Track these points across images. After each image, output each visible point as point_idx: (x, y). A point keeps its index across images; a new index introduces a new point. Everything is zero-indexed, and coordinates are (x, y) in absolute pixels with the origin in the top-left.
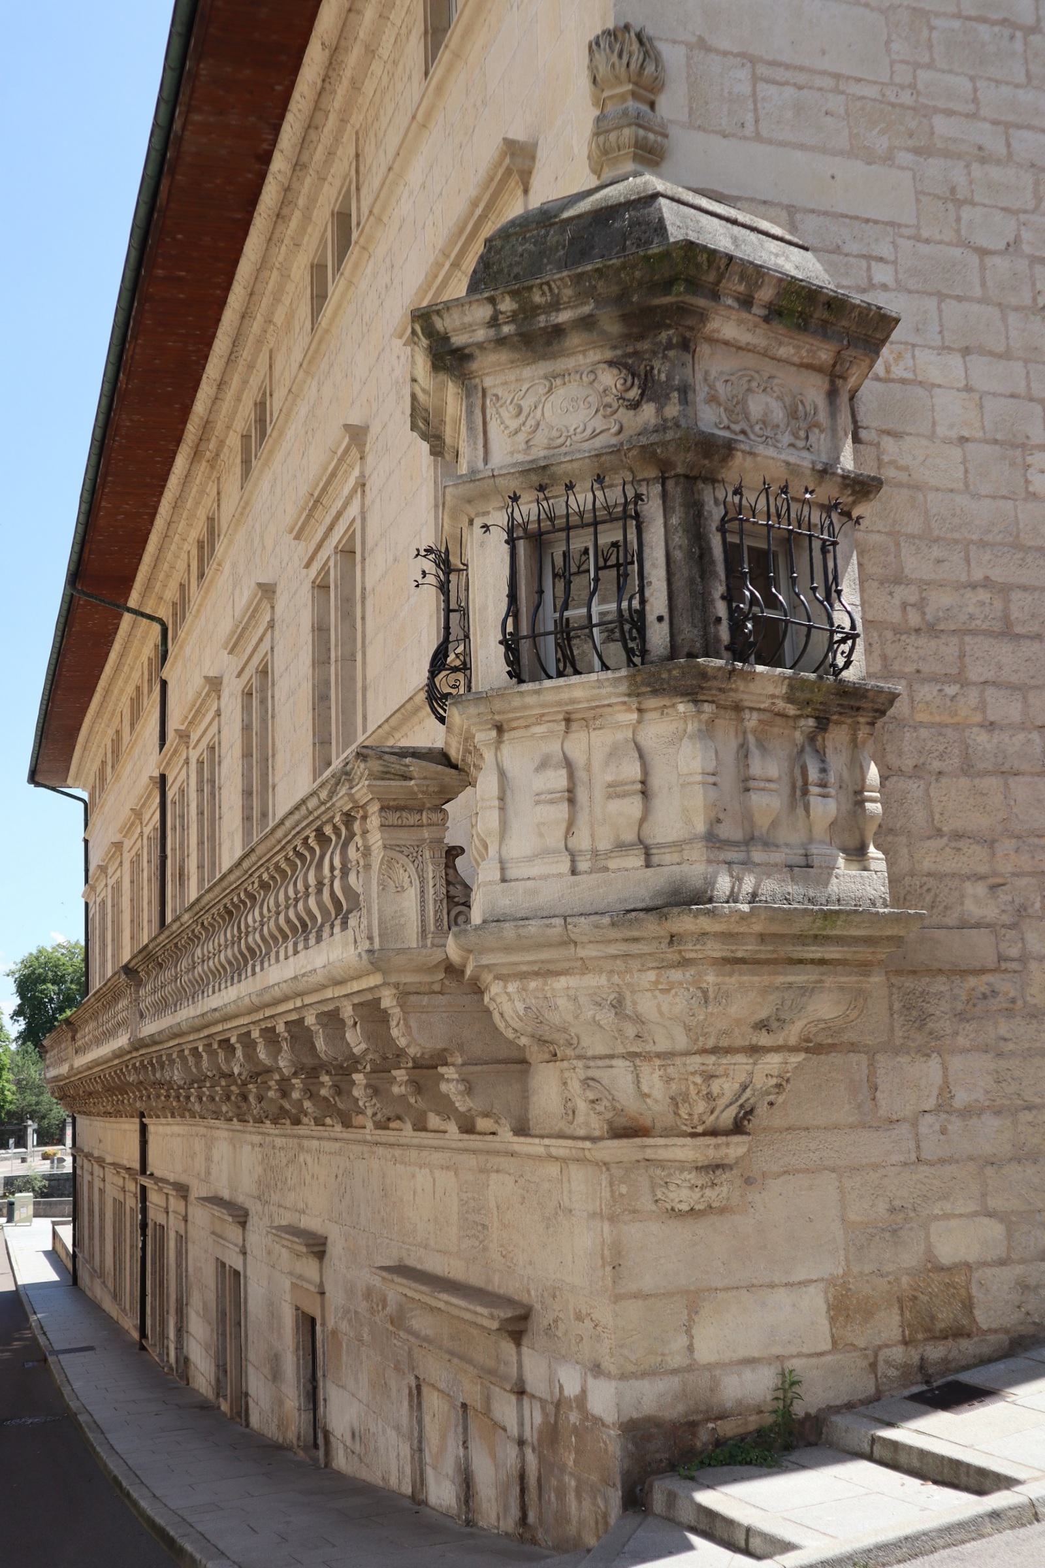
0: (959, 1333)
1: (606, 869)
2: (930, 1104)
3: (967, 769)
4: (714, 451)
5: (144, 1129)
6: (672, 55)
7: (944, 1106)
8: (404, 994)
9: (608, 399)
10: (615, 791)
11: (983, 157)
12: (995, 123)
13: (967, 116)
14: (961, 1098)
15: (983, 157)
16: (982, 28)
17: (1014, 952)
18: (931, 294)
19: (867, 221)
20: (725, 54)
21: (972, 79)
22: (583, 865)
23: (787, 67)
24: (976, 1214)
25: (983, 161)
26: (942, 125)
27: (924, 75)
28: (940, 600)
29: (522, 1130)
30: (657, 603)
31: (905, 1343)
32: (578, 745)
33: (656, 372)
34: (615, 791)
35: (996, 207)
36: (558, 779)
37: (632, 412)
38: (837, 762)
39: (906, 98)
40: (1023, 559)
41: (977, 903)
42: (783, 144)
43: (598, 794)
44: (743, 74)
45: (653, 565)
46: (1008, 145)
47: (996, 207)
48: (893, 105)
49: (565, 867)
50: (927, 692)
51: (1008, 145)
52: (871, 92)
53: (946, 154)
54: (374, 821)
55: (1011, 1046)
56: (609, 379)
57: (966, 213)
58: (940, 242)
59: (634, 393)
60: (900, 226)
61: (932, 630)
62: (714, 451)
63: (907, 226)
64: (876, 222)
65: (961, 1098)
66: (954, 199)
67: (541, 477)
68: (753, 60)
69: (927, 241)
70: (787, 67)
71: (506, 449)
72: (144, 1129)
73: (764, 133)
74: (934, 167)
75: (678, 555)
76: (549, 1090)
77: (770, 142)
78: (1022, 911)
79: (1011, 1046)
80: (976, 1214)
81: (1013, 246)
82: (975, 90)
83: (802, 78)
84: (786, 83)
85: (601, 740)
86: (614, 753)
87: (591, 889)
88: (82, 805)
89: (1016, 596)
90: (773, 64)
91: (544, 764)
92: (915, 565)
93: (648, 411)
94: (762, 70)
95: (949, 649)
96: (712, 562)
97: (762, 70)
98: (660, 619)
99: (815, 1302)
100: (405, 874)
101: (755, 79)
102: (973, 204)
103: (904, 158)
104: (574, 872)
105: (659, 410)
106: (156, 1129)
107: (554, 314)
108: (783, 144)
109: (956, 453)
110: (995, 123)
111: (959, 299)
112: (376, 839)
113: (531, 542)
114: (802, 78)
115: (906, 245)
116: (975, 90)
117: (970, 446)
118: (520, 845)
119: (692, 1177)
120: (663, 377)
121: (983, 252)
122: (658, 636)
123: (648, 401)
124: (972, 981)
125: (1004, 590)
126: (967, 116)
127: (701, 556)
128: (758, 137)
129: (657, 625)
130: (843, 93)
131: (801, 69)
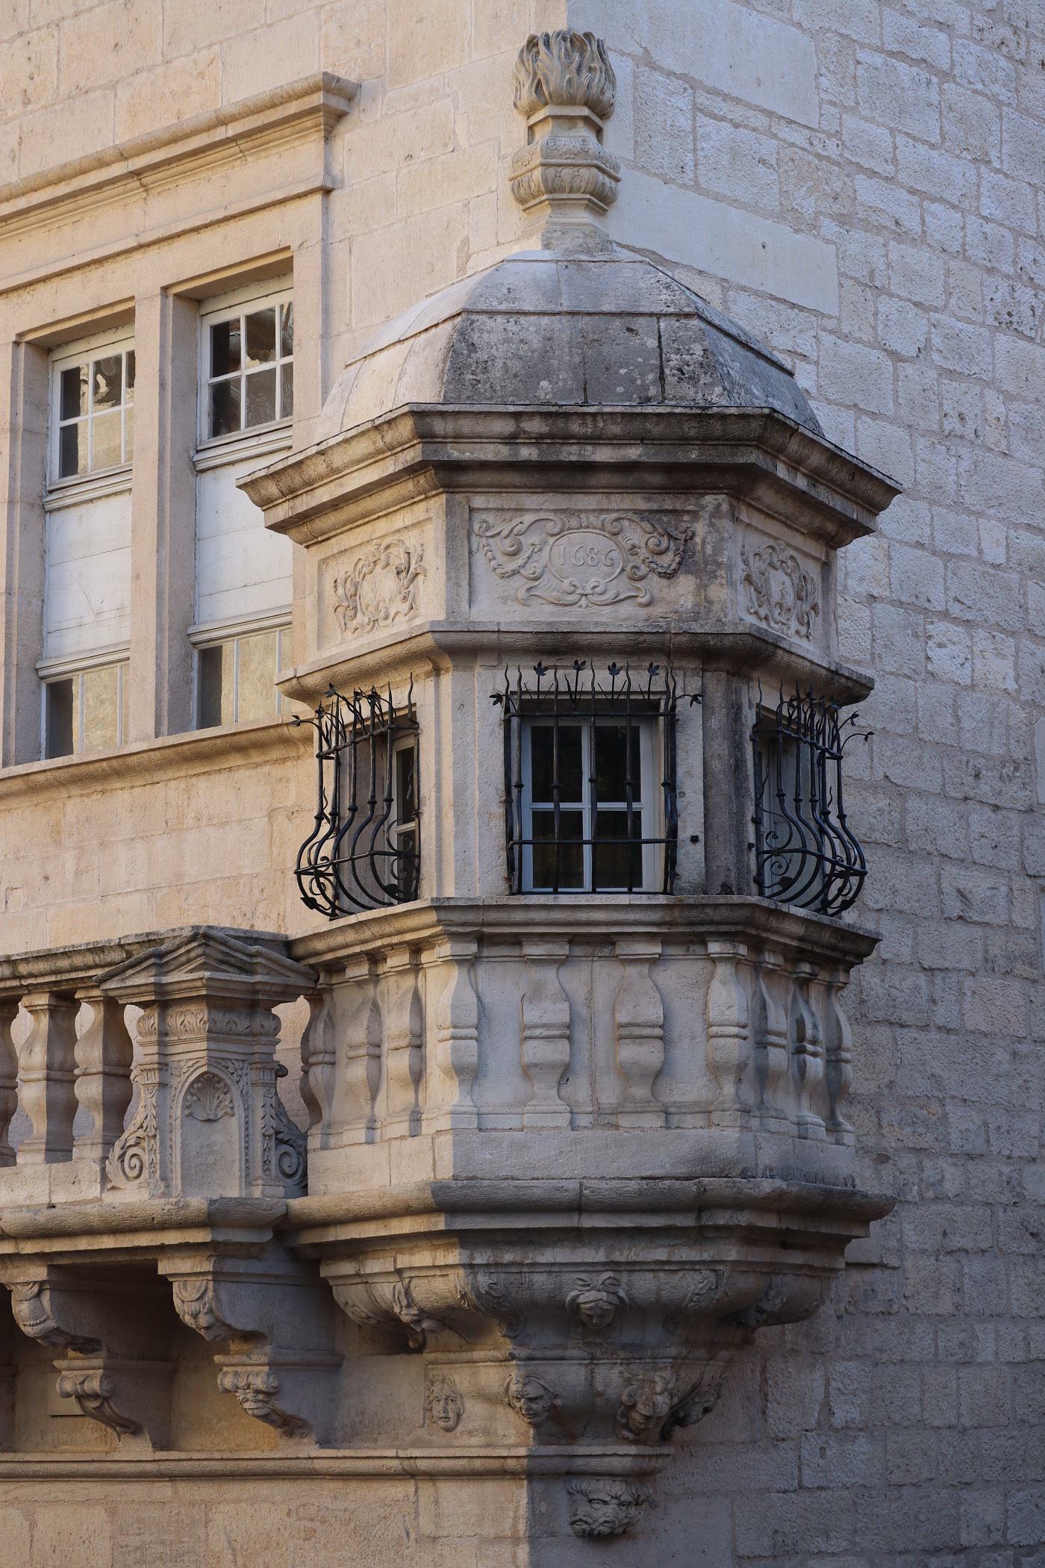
1: (617, 1127)
2: (812, 1422)
7: (826, 1424)
9: (637, 561)
11: (899, 232)
12: (913, 191)
13: (887, 179)
14: (839, 1417)
15: (899, 232)
16: (902, 67)
17: (893, 1244)
18: (848, 407)
19: (793, 306)
20: (670, 74)
21: (892, 131)
22: (583, 1120)
23: (726, 97)
24: (846, 1552)
25: (900, 238)
26: (867, 191)
27: (850, 122)
33: (698, 540)
35: (910, 300)
37: (665, 582)
39: (832, 150)
40: (920, 758)
42: (719, 198)
43: (603, 1037)
44: (683, 102)
45: (689, 774)
46: (923, 222)
47: (910, 300)
48: (819, 156)
49: (563, 1120)
51: (923, 222)
52: (799, 137)
53: (868, 227)
55: (885, 1357)
57: (885, 305)
58: (859, 341)
59: (668, 560)
60: (823, 315)
63: (830, 317)
64: (802, 309)
65: (839, 1417)
68: (692, 84)
69: (846, 337)
70: (726, 97)
73: (702, 181)
74: (857, 241)
75: (716, 765)
77: (706, 193)
79: (885, 1357)
80: (846, 1552)
82: (895, 148)
83: (738, 113)
84: (722, 119)
89: (913, 803)
90: (714, 92)
94: (703, 99)
96: (746, 778)
97: (703, 99)
98: (694, 839)
101: (697, 109)
102: (891, 295)
104: (573, 1126)
105: (701, 587)
107: (589, 448)
108: (719, 198)
109: (865, 613)
110: (913, 191)
111: (874, 415)
114: (738, 113)
115: (828, 339)
116: (895, 148)
117: (879, 606)
119: (618, 1488)
120: (709, 550)
121: (895, 356)
123: (687, 572)
126: (887, 179)
128: (696, 187)
129: (690, 846)
130: (774, 136)
131: (738, 101)
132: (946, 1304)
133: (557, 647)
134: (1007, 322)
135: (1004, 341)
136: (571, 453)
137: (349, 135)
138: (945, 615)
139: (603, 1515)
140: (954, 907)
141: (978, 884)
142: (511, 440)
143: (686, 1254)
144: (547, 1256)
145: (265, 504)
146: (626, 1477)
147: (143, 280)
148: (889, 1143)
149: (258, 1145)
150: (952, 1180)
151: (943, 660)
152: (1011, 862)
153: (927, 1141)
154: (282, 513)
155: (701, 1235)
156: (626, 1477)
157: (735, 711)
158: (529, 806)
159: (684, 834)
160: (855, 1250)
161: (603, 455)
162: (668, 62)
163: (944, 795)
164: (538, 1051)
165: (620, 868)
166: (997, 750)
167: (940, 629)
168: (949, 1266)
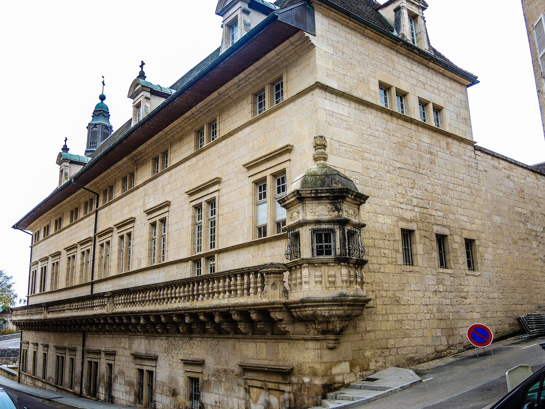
0: (367, 370)
16: (371, 137)
26: (366, 155)
31: (360, 371)
39: (361, 149)
43: (327, 276)
44: (338, 144)
57: (369, 171)
68: (339, 142)
74: (365, 162)
83: (346, 145)
88: (31, 236)
89: (376, 241)
94: (341, 144)
97: (341, 144)
103: (360, 160)
113: (314, 231)
114: (346, 145)
119: (333, 342)
124: (370, 309)
125: (374, 239)
128: (340, 156)
132: (384, 312)
133: (318, 222)
134: (388, 172)
135: (388, 174)
136: (319, 195)
138: (380, 214)
139: (331, 345)
140: (383, 255)
141: (386, 251)
142: (310, 193)
143: (340, 308)
144: (320, 308)
145: (280, 204)
146: (334, 340)
147: (268, 173)
148: (374, 289)
149: (281, 293)
150: (384, 294)
152: (392, 248)
153: (380, 288)
154: (282, 204)
155: (342, 305)
156: (334, 340)
157: (344, 230)
158: (315, 244)
159: (337, 248)
160: (367, 305)
161: (323, 195)
162: (335, 139)
163: (380, 239)
164: (317, 279)
165: (329, 253)
166: (389, 232)
167: (379, 216)
168: (384, 307)
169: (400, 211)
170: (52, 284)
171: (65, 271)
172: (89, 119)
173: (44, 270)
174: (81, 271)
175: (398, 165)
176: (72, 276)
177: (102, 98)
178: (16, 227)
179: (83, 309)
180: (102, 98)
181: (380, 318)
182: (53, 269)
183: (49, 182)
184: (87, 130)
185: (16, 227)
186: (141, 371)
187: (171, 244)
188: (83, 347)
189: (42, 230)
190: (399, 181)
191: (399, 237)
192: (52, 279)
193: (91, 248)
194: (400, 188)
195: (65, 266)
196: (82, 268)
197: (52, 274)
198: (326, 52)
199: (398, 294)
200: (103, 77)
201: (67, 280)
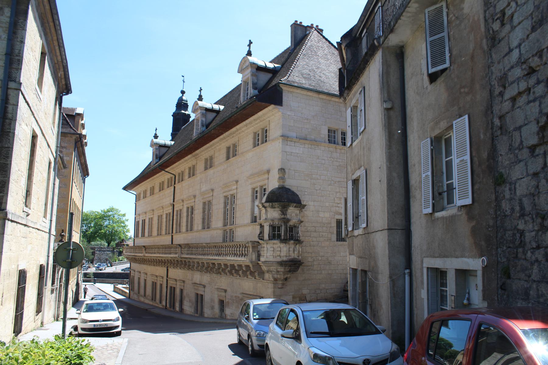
3: (310, 246)
4: (288, 220)
5: (167, 270)
6: (287, 171)
8: (253, 266)
10: (278, 251)
28: (309, 228)
29: (263, 279)
30: (283, 234)
32: (274, 246)
34: (278, 251)
36: (272, 249)
38: (297, 248)
41: (310, 259)
50: (307, 238)
54: (251, 248)
56: (280, 212)
61: (308, 231)
62: (288, 220)
66: (314, 184)
67: (273, 220)
71: (269, 216)
72: (167, 270)
76: (267, 276)
78: (314, 260)
81: (320, 189)
85: (277, 246)
86: (278, 247)
87: (275, 260)
91: (271, 247)
92: (307, 225)
93: (283, 216)
95: (309, 233)
99: (291, 297)
100: (254, 253)
106: (170, 270)
112: (251, 250)
113: (271, 226)
118: (268, 254)
122: (283, 237)
125: (315, 227)
127: (287, 228)
137: (270, 174)
141: (324, 234)
150: (320, 258)
151: (320, 215)
169: (337, 208)
170: (149, 232)
171: (157, 224)
172: (174, 109)
173: (144, 221)
174: (166, 226)
175: (338, 180)
176: (161, 229)
177: (183, 92)
178: (125, 188)
179: (165, 253)
180: (183, 92)
181: (316, 272)
182: (149, 222)
183: (146, 157)
184: (172, 118)
185: (125, 188)
186: (197, 294)
187: (214, 217)
188: (167, 277)
189: (142, 193)
190: (338, 190)
191: (334, 224)
192: (149, 229)
193: (171, 211)
194: (338, 194)
195: (157, 221)
196: (166, 224)
197: (149, 225)
198: (289, 115)
199: (330, 259)
200: (183, 76)
201: (158, 230)
